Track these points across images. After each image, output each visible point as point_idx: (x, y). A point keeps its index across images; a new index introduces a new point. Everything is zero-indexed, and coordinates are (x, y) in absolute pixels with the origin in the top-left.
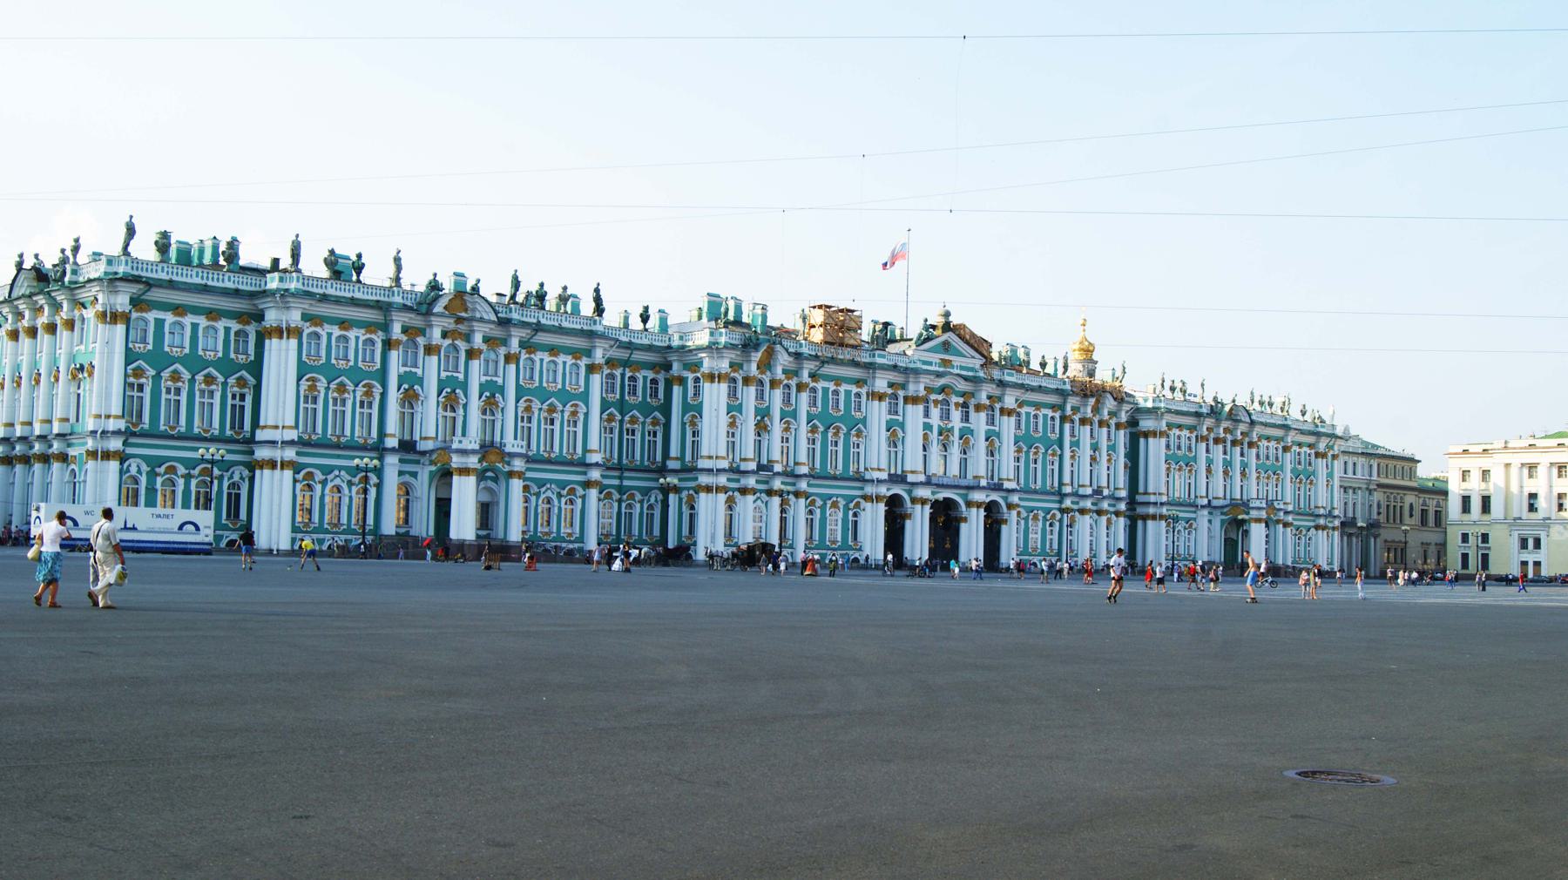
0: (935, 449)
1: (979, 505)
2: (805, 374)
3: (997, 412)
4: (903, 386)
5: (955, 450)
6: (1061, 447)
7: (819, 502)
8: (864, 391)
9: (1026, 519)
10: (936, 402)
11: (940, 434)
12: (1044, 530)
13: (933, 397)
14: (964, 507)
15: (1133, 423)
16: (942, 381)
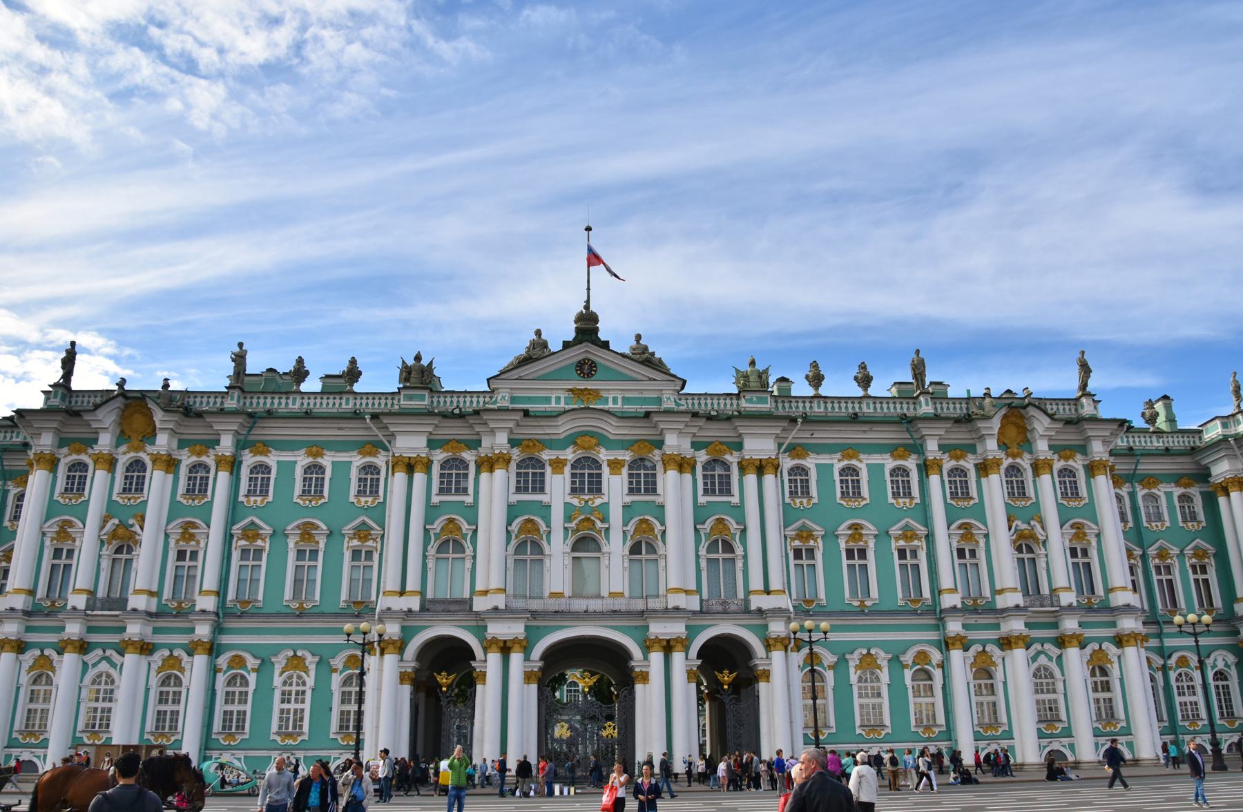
0: (558, 547)
1: (668, 647)
2: (227, 444)
3: (735, 470)
4: (475, 444)
5: (616, 546)
6: (927, 520)
7: (251, 662)
8: (380, 460)
9: (840, 666)
10: (558, 465)
11: (568, 518)
12: (896, 687)
13: (546, 455)
14: (636, 652)
15: (1203, 475)
16: (563, 428)
